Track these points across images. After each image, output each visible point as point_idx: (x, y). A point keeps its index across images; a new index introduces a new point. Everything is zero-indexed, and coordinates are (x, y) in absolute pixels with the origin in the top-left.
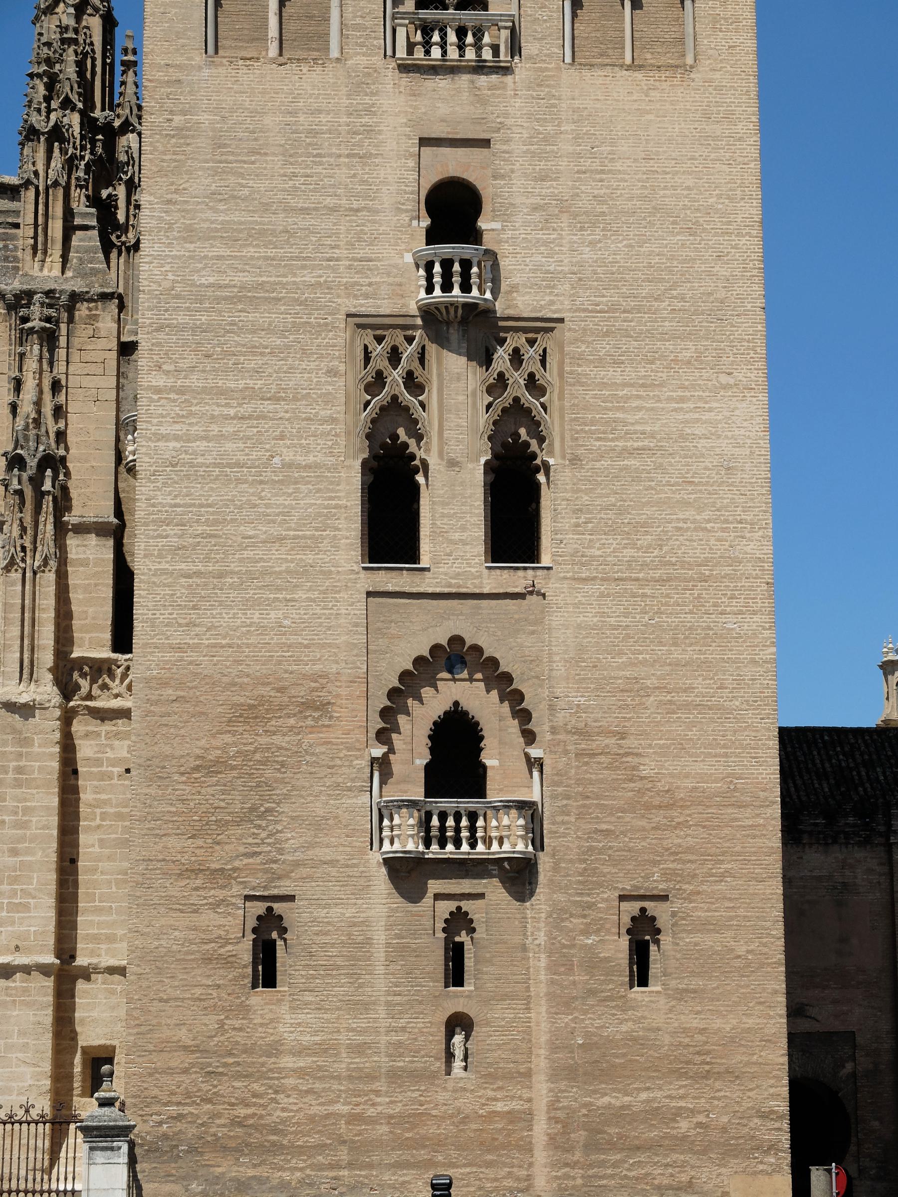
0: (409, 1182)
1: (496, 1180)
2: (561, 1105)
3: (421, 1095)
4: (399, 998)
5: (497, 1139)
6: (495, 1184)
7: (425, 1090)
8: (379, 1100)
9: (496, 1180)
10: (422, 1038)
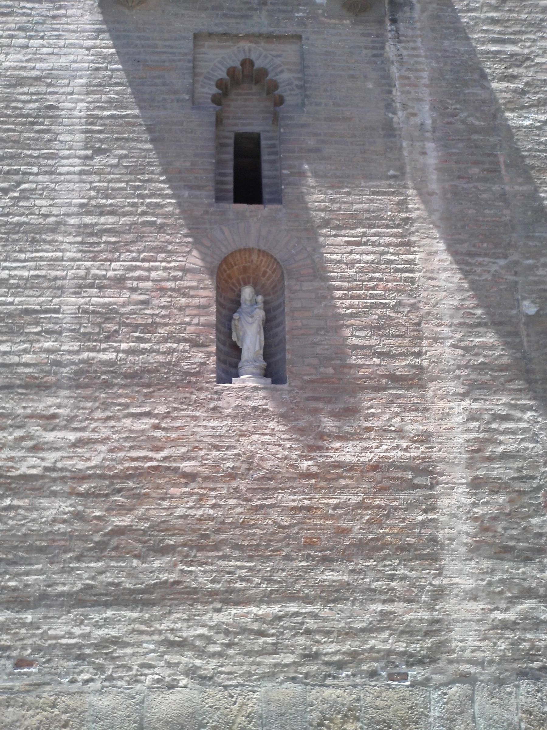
0: (116, 642)
1: (350, 633)
2: (500, 449)
3: (156, 427)
4: (111, 219)
5: (345, 532)
6: (349, 645)
7: (167, 415)
8: (50, 436)
9: (350, 633)
10: (163, 301)
